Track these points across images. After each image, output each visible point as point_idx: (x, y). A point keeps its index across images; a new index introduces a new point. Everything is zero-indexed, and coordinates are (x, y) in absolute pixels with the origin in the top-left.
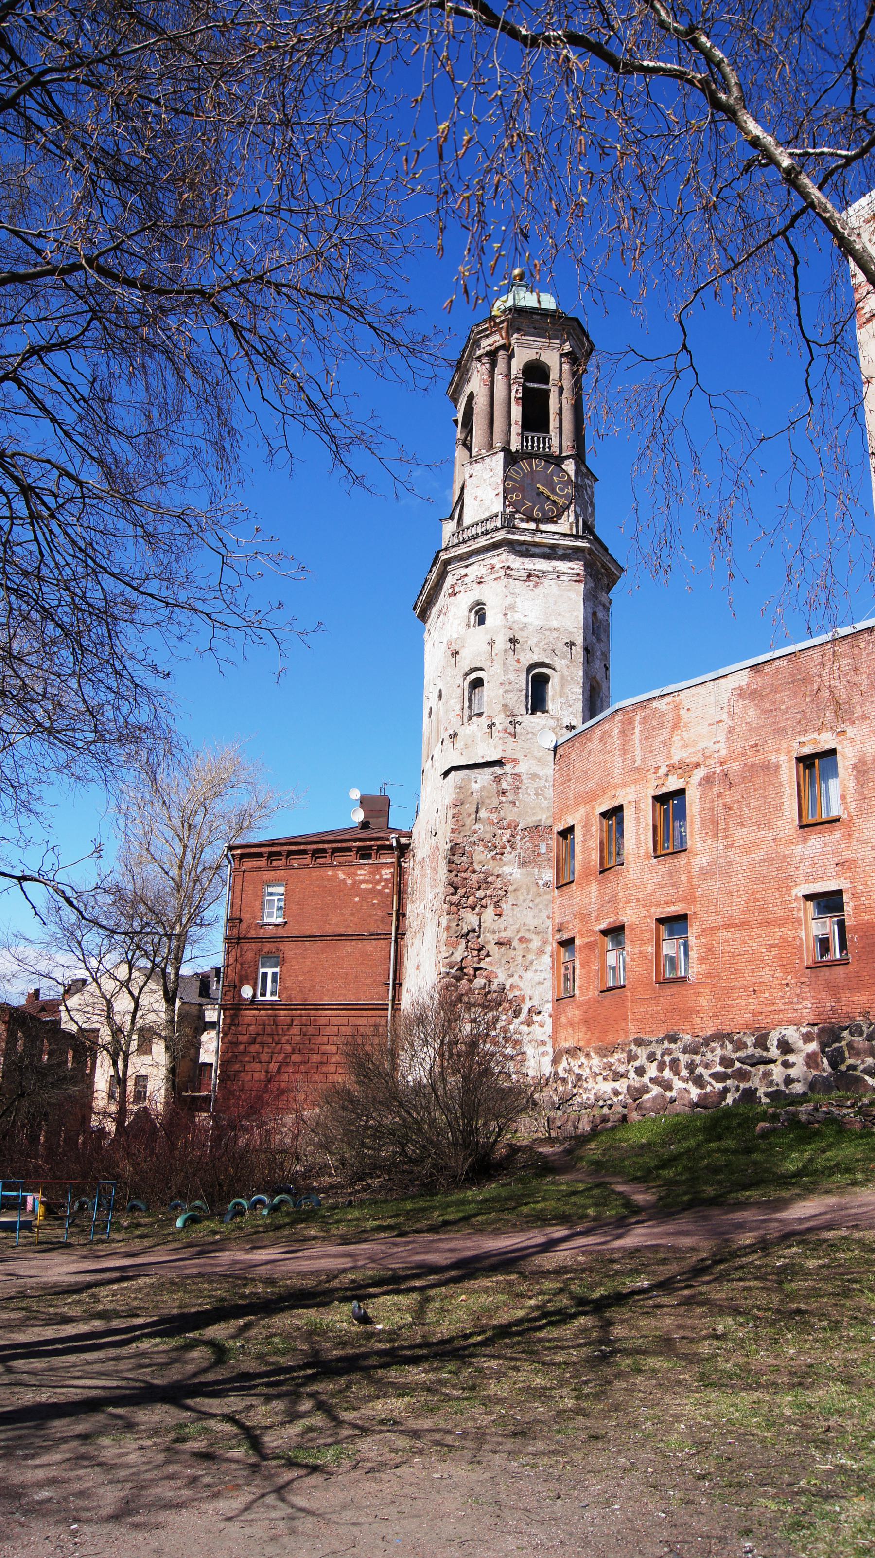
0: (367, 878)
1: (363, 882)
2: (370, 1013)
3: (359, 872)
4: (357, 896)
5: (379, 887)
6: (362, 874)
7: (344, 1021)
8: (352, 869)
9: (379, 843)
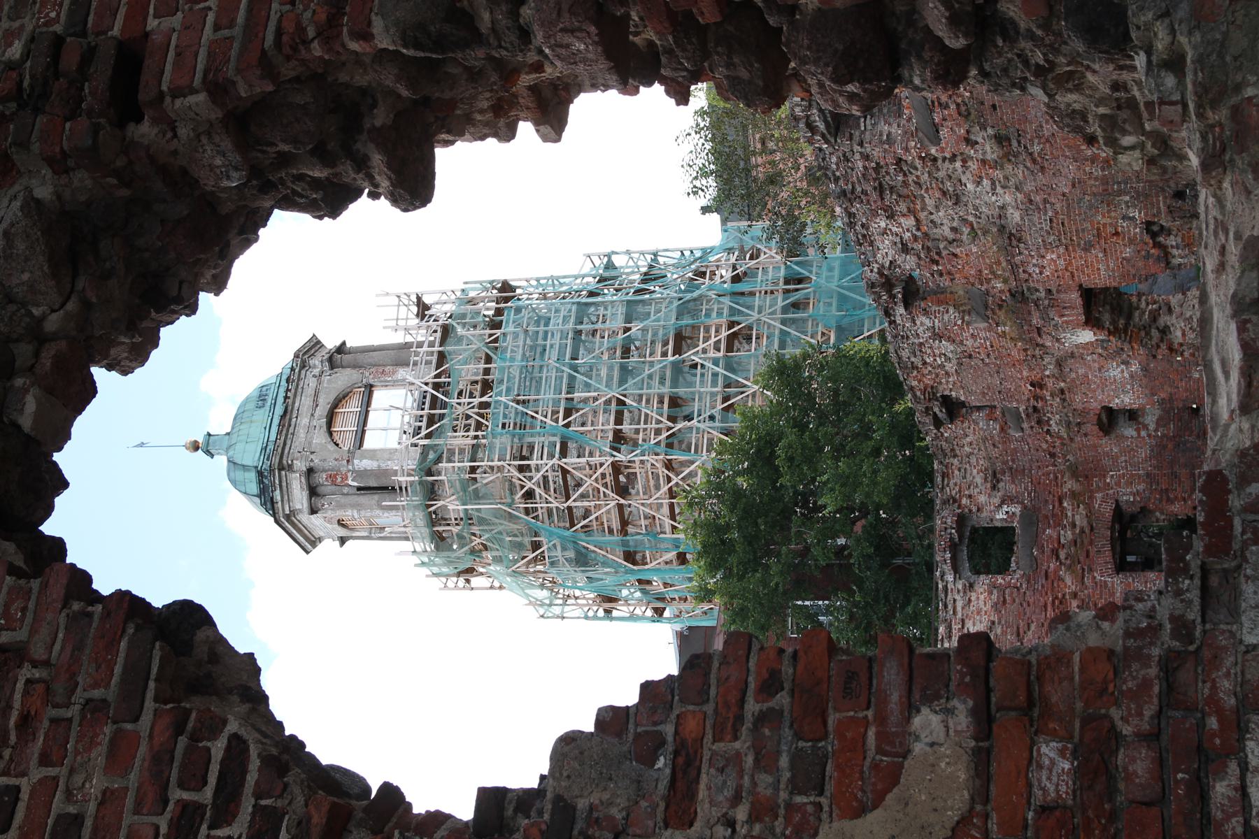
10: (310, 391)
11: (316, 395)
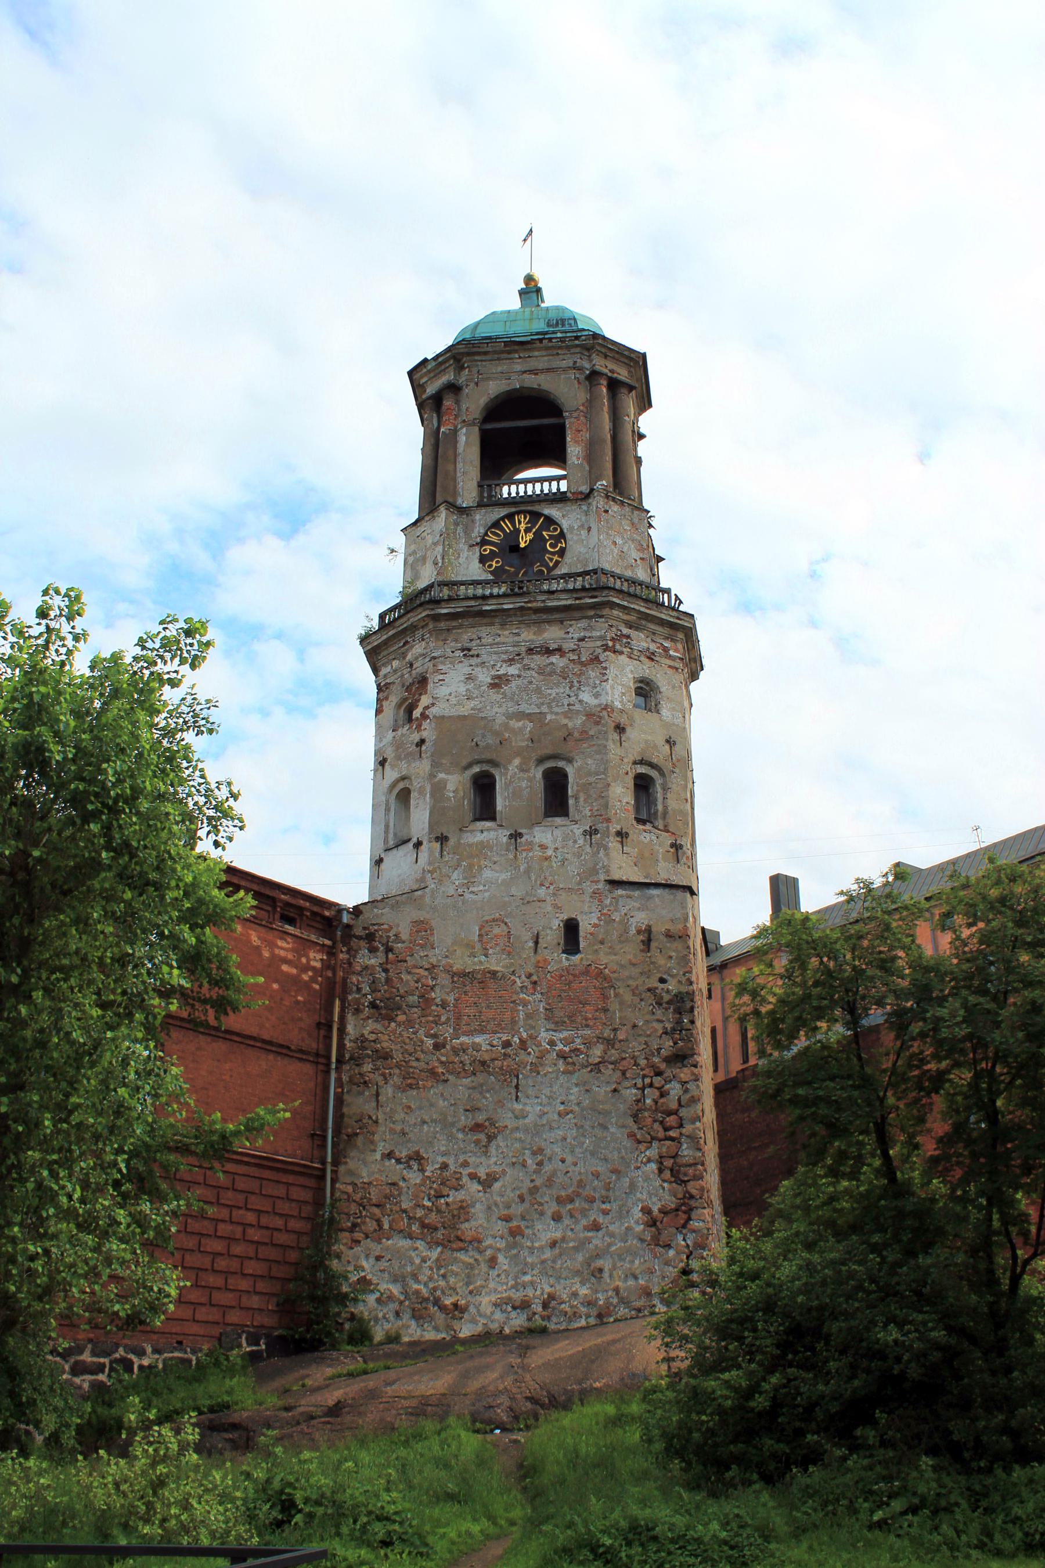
0: (290, 956)
2: (291, 1178)
3: (280, 943)
4: (276, 981)
5: (305, 977)
6: (284, 947)
7: (254, 1185)
8: (270, 936)
9: (315, 909)
10: (557, 363)
11: (549, 370)
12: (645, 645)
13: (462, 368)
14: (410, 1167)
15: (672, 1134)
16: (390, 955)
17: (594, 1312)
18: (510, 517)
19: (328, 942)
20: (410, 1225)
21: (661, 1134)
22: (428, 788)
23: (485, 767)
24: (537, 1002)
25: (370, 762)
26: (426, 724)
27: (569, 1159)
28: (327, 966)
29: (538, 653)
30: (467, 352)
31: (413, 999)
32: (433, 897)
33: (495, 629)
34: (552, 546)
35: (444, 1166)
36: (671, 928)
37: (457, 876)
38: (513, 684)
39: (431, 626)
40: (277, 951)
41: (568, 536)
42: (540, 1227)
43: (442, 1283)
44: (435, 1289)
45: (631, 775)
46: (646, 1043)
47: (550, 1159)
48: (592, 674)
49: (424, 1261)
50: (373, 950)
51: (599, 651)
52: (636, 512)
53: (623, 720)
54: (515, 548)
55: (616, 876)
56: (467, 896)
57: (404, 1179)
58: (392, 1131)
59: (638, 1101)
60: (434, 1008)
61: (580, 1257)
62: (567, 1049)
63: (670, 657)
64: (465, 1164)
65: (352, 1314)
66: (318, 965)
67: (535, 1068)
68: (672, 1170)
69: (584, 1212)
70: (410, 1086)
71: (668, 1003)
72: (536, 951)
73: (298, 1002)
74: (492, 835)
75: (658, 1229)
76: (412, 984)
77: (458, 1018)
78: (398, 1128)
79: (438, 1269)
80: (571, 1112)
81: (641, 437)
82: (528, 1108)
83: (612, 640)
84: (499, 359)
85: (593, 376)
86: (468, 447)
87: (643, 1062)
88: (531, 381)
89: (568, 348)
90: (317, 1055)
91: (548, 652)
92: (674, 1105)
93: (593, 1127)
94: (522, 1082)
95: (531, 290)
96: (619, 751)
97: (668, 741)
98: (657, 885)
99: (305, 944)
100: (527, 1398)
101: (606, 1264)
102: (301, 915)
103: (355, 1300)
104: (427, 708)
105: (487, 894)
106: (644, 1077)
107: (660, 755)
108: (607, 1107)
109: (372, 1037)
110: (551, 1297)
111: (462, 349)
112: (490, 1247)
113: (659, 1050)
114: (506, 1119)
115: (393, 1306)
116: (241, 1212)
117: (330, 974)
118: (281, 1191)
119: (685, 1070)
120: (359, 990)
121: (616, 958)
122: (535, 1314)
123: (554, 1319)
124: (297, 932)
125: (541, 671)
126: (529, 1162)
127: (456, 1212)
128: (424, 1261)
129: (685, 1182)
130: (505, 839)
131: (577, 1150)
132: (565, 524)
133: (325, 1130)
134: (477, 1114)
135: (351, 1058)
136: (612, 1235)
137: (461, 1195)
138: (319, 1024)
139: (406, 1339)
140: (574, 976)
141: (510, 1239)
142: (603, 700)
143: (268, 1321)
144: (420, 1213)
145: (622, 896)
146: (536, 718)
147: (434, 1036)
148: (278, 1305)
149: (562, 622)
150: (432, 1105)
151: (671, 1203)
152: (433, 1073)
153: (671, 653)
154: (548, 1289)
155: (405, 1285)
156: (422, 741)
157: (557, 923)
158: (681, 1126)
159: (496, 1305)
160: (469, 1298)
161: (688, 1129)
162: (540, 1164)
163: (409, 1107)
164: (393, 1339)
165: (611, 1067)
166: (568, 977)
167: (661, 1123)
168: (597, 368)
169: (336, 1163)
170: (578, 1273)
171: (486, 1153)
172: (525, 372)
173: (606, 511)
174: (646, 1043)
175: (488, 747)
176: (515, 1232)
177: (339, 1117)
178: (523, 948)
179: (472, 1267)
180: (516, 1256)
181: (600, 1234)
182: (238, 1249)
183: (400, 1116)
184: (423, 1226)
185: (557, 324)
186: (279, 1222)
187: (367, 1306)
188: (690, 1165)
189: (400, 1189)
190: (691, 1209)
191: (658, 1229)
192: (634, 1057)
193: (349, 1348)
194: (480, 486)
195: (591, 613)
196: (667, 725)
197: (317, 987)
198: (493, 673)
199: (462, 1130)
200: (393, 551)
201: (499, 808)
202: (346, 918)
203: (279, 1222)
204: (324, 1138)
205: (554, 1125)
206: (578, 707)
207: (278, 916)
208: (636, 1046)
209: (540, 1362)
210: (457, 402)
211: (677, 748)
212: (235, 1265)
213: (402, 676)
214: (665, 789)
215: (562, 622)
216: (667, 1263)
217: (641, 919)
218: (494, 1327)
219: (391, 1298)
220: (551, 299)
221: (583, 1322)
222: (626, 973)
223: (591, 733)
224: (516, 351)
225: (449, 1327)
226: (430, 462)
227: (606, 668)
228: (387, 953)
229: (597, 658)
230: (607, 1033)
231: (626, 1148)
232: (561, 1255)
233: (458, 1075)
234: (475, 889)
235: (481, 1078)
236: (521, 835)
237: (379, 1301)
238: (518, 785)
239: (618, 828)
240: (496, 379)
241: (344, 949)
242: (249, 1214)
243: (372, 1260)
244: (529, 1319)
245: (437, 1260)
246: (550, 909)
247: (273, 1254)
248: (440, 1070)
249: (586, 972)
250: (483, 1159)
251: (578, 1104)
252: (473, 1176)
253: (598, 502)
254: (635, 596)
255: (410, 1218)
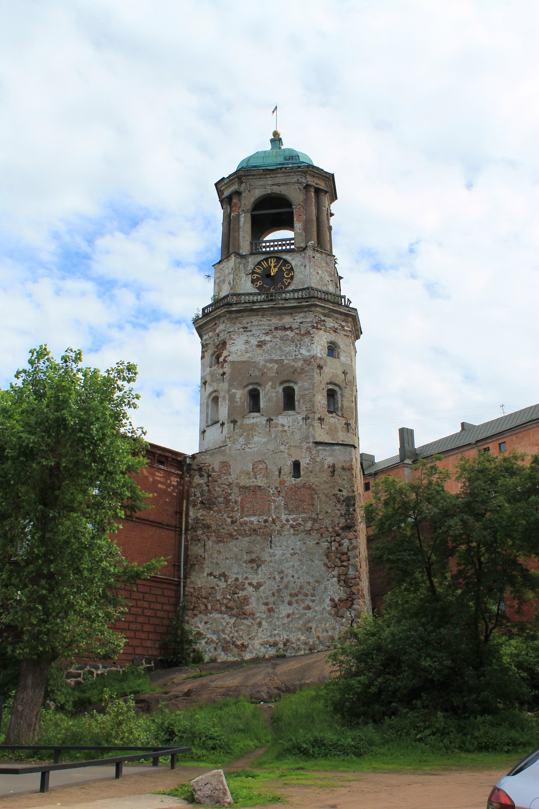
0: (162, 480)
1: (160, 482)
2: (164, 586)
3: (157, 474)
9: (174, 457)
10: (289, 180)
11: (285, 184)
12: (332, 325)
13: (242, 183)
14: (220, 580)
15: (345, 564)
16: (210, 478)
17: (307, 647)
18: (266, 260)
19: (180, 473)
20: (221, 607)
21: (339, 564)
22: (227, 397)
23: (255, 387)
24: (280, 501)
25: (199, 382)
26: (226, 365)
27: (296, 576)
28: (179, 484)
29: (280, 329)
30: (245, 174)
31: (221, 500)
32: (230, 449)
33: (259, 318)
34: (287, 274)
35: (237, 579)
36: (345, 465)
37: (241, 440)
38: (268, 345)
39: (228, 316)
40: (156, 478)
41: (295, 270)
42: (282, 608)
43: (236, 634)
44: (233, 637)
45: (326, 390)
46: (332, 521)
47: (287, 576)
48: (307, 340)
49: (227, 624)
50: (201, 476)
51: (310, 328)
52: (328, 257)
53: (322, 363)
54: (269, 276)
55: (318, 440)
56: (247, 449)
57: (218, 586)
58: (212, 562)
59: (328, 548)
60: (231, 504)
61: (301, 622)
62: (295, 523)
63: (345, 330)
64: (247, 578)
65: (194, 649)
66: (175, 483)
67: (279, 533)
68: (344, 581)
69: (303, 601)
70: (220, 541)
71: (343, 501)
72: (279, 477)
73: (166, 502)
74: (258, 420)
75: (338, 609)
76: (221, 492)
77: (242, 509)
78: (215, 561)
79: (234, 628)
80: (297, 553)
81: (332, 215)
82: (276, 552)
83: (316, 323)
84: (260, 178)
85: (307, 187)
86: (245, 223)
87: (330, 530)
88: (276, 190)
89: (295, 172)
90: (176, 527)
91: (285, 329)
92: (345, 550)
93: (307, 561)
94: (273, 539)
95: (276, 140)
96: (320, 379)
97: (343, 373)
98: (338, 444)
99: (168, 474)
100: (275, 688)
101: (313, 625)
102: (167, 460)
103: (196, 643)
104: (226, 357)
105: (256, 449)
106: (331, 537)
107: (340, 379)
108: (313, 551)
109: (202, 518)
110: (288, 641)
111: (241, 173)
112: (259, 617)
113: (338, 524)
114: (265, 556)
115: (213, 645)
116: (141, 602)
117: (181, 488)
118: (159, 592)
119: (351, 533)
120: (195, 495)
121: (318, 479)
122: (280, 648)
123: (289, 651)
124: (165, 468)
125: (282, 339)
126: (277, 577)
127: (242, 601)
128: (227, 624)
129: (351, 587)
130: (264, 422)
131: (300, 572)
132: (293, 263)
133: (180, 563)
134: (252, 554)
135: (192, 528)
136: (316, 612)
137: (244, 593)
138: (176, 512)
139: (219, 661)
140: (298, 488)
141: (268, 613)
142: (312, 353)
143: (155, 652)
144: (225, 601)
145: (320, 449)
146: (279, 362)
147: (232, 517)
148: (160, 645)
149: (292, 314)
150: (230, 550)
151: (344, 596)
152: (231, 535)
153: (346, 328)
154: (286, 637)
155: (219, 636)
156: (224, 374)
157: (289, 463)
158: (349, 560)
159: (261, 644)
160: (249, 641)
161: (352, 561)
162: (282, 578)
163: (220, 551)
164: (213, 660)
165: (315, 532)
166: (295, 489)
167: (339, 558)
168: (310, 183)
169: (185, 578)
170: (300, 629)
171: (256, 573)
172: (273, 185)
173: (314, 257)
174: (332, 521)
175: (256, 376)
176: (270, 610)
177: (186, 556)
178: (273, 475)
179: (249, 626)
180: (271, 621)
181: (311, 611)
182: (140, 619)
183: (215, 555)
184: (227, 607)
185: (289, 159)
186: (159, 607)
187: (201, 646)
188: (353, 579)
189: (216, 590)
190: (354, 600)
191: (338, 609)
192: (326, 527)
193: (193, 665)
194: (251, 244)
195: (306, 310)
196: (343, 364)
197: (175, 494)
198: (258, 340)
199: (245, 562)
200: (208, 276)
201: (261, 406)
202: (188, 461)
203: (159, 607)
204: (180, 566)
205: (289, 560)
206: (299, 356)
207: (156, 461)
208: (327, 522)
209: (282, 671)
210: (240, 200)
211: (348, 376)
212: (139, 627)
213: (214, 340)
214: (342, 396)
215: (292, 314)
216: (342, 625)
217: (329, 460)
218: (261, 655)
219: (212, 641)
220: (286, 145)
221: (302, 652)
222: (323, 487)
223: (306, 369)
224: (269, 174)
225: (240, 655)
226: (226, 231)
227: (313, 337)
228: (208, 477)
229: (309, 332)
230: (314, 515)
231: (323, 571)
232: (292, 621)
233: (243, 536)
234: (250, 446)
235: (253, 537)
236: (272, 420)
237: (206, 643)
238: (270, 395)
239: (319, 416)
240: (259, 188)
241: (188, 476)
242: (145, 603)
243: (203, 624)
244: (277, 651)
245: (234, 623)
246: (286, 456)
247: (157, 621)
248: (234, 534)
249: (304, 486)
250: (255, 576)
251: (300, 550)
252: (250, 584)
253: (309, 252)
254: (328, 301)
255: (220, 604)
